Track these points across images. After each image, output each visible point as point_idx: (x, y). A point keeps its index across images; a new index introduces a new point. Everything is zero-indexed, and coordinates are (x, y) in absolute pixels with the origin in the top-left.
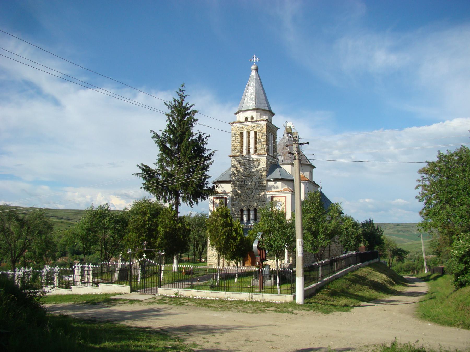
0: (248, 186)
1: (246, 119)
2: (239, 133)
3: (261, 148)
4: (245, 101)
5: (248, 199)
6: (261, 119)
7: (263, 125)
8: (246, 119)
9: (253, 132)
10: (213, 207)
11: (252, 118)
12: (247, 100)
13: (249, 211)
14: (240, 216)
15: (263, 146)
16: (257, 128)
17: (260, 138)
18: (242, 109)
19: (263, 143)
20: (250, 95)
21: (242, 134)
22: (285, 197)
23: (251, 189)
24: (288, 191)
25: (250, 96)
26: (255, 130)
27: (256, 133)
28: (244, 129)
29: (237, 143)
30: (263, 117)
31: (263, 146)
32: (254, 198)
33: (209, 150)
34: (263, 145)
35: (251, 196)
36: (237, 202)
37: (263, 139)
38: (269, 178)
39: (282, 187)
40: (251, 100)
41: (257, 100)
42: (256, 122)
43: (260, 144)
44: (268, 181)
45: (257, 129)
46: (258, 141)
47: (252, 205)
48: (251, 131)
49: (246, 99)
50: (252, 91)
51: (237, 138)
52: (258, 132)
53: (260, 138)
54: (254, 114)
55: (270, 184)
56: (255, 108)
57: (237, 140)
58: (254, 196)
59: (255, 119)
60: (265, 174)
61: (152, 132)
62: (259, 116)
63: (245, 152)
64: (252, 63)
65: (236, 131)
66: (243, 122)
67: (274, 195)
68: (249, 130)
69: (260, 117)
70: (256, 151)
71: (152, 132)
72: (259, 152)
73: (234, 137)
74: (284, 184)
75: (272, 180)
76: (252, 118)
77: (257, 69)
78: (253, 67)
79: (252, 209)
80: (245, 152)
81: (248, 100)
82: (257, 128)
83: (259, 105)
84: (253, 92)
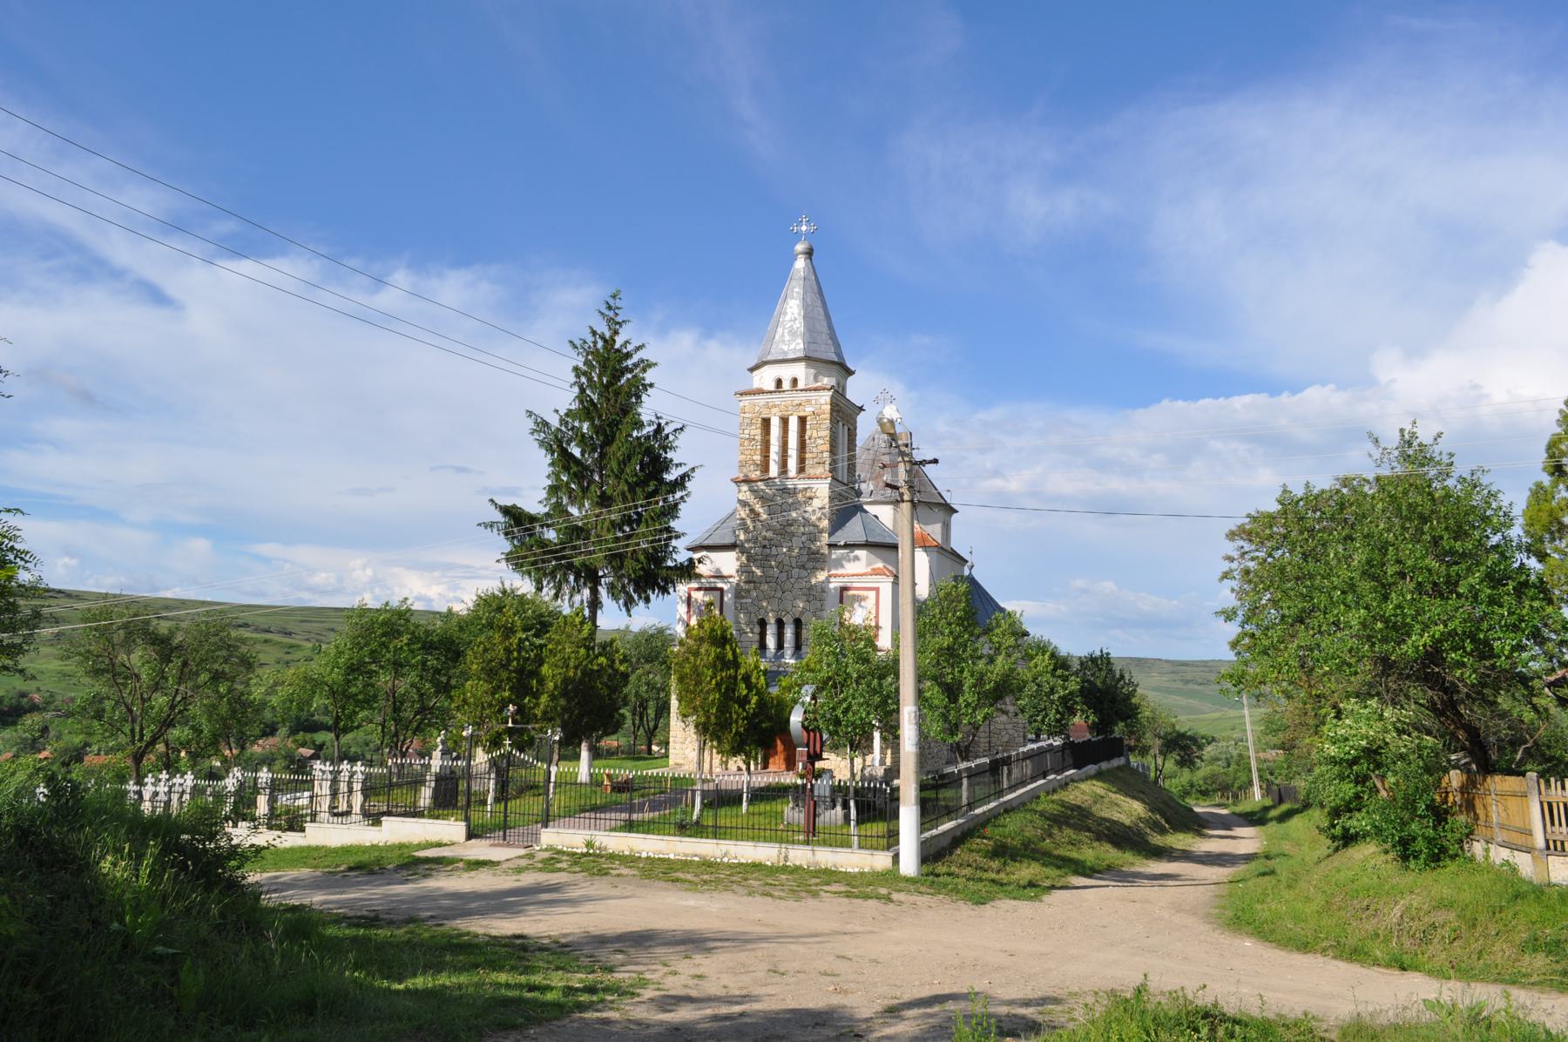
1: (779, 382)
4: (777, 337)
5: (779, 594)
6: (819, 384)
7: (823, 402)
8: (779, 382)
10: (688, 612)
11: (795, 381)
12: (783, 335)
13: (780, 624)
14: (757, 637)
15: (820, 455)
16: (807, 409)
17: (815, 435)
18: (769, 358)
19: (820, 448)
21: (766, 423)
22: (877, 590)
24: (885, 574)
25: (789, 325)
26: (802, 414)
27: (803, 421)
28: (774, 410)
30: (822, 381)
33: (681, 464)
34: (822, 452)
35: (787, 586)
36: (750, 601)
38: (834, 539)
39: (869, 564)
40: (793, 333)
41: (807, 334)
42: (803, 394)
44: (832, 546)
45: (808, 410)
46: (808, 441)
47: (789, 608)
48: (790, 418)
49: (780, 330)
51: (753, 432)
52: (808, 418)
53: (815, 435)
54: (800, 371)
55: (836, 553)
56: (801, 354)
59: (801, 385)
60: (825, 523)
61: (530, 416)
62: (812, 377)
63: (774, 470)
64: (797, 237)
66: (771, 392)
67: (849, 585)
68: (786, 413)
69: (816, 379)
70: (801, 470)
71: (530, 416)
72: (810, 471)
73: (746, 432)
74: (873, 556)
75: (842, 543)
76: (795, 381)
77: (809, 253)
78: (800, 247)
79: (788, 619)
80: (774, 470)
81: (786, 334)
83: (813, 347)
84: (799, 314)
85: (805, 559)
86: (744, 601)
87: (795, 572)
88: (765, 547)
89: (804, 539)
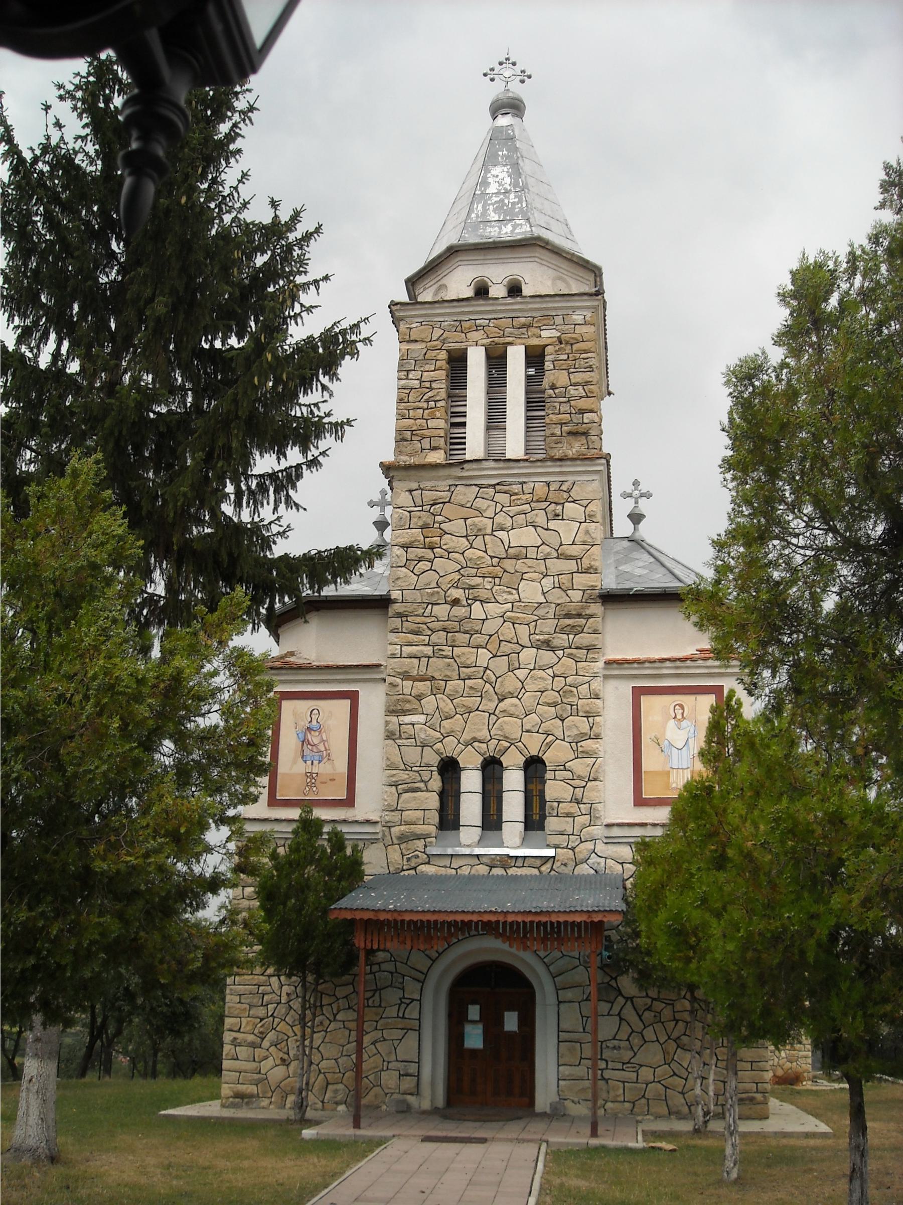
0: (490, 627)
1: (482, 291)
2: (443, 355)
3: (565, 428)
8: (482, 291)
9: (522, 349)
11: (515, 290)
15: (577, 418)
20: (498, 193)
23: (506, 648)
25: (495, 199)
26: (535, 342)
27: (535, 358)
29: (432, 404)
31: (577, 418)
32: (528, 699)
36: (421, 718)
37: (575, 385)
43: (565, 408)
48: (510, 349)
50: (508, 180)
52: (549, 350)
57: (431, 389)
58: (530, 686)
65: (423, 345)
66: (467, 299)
68: (502, 340)
79: (513, 761)
82: (544, 334)
85: (548, 626)
86: (407, 719)
87: (528, 655)
88: (456, 602)
89: (548, 583)
